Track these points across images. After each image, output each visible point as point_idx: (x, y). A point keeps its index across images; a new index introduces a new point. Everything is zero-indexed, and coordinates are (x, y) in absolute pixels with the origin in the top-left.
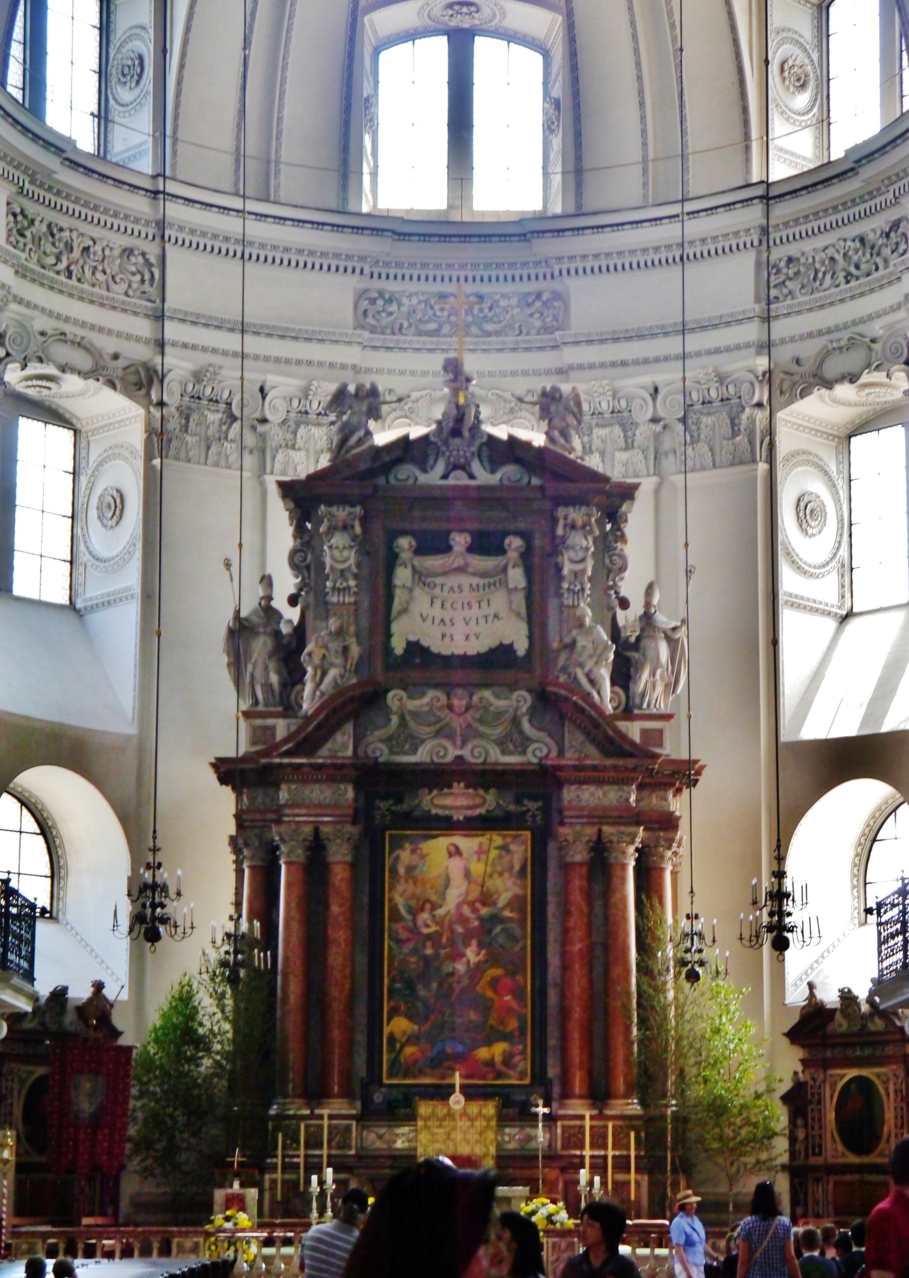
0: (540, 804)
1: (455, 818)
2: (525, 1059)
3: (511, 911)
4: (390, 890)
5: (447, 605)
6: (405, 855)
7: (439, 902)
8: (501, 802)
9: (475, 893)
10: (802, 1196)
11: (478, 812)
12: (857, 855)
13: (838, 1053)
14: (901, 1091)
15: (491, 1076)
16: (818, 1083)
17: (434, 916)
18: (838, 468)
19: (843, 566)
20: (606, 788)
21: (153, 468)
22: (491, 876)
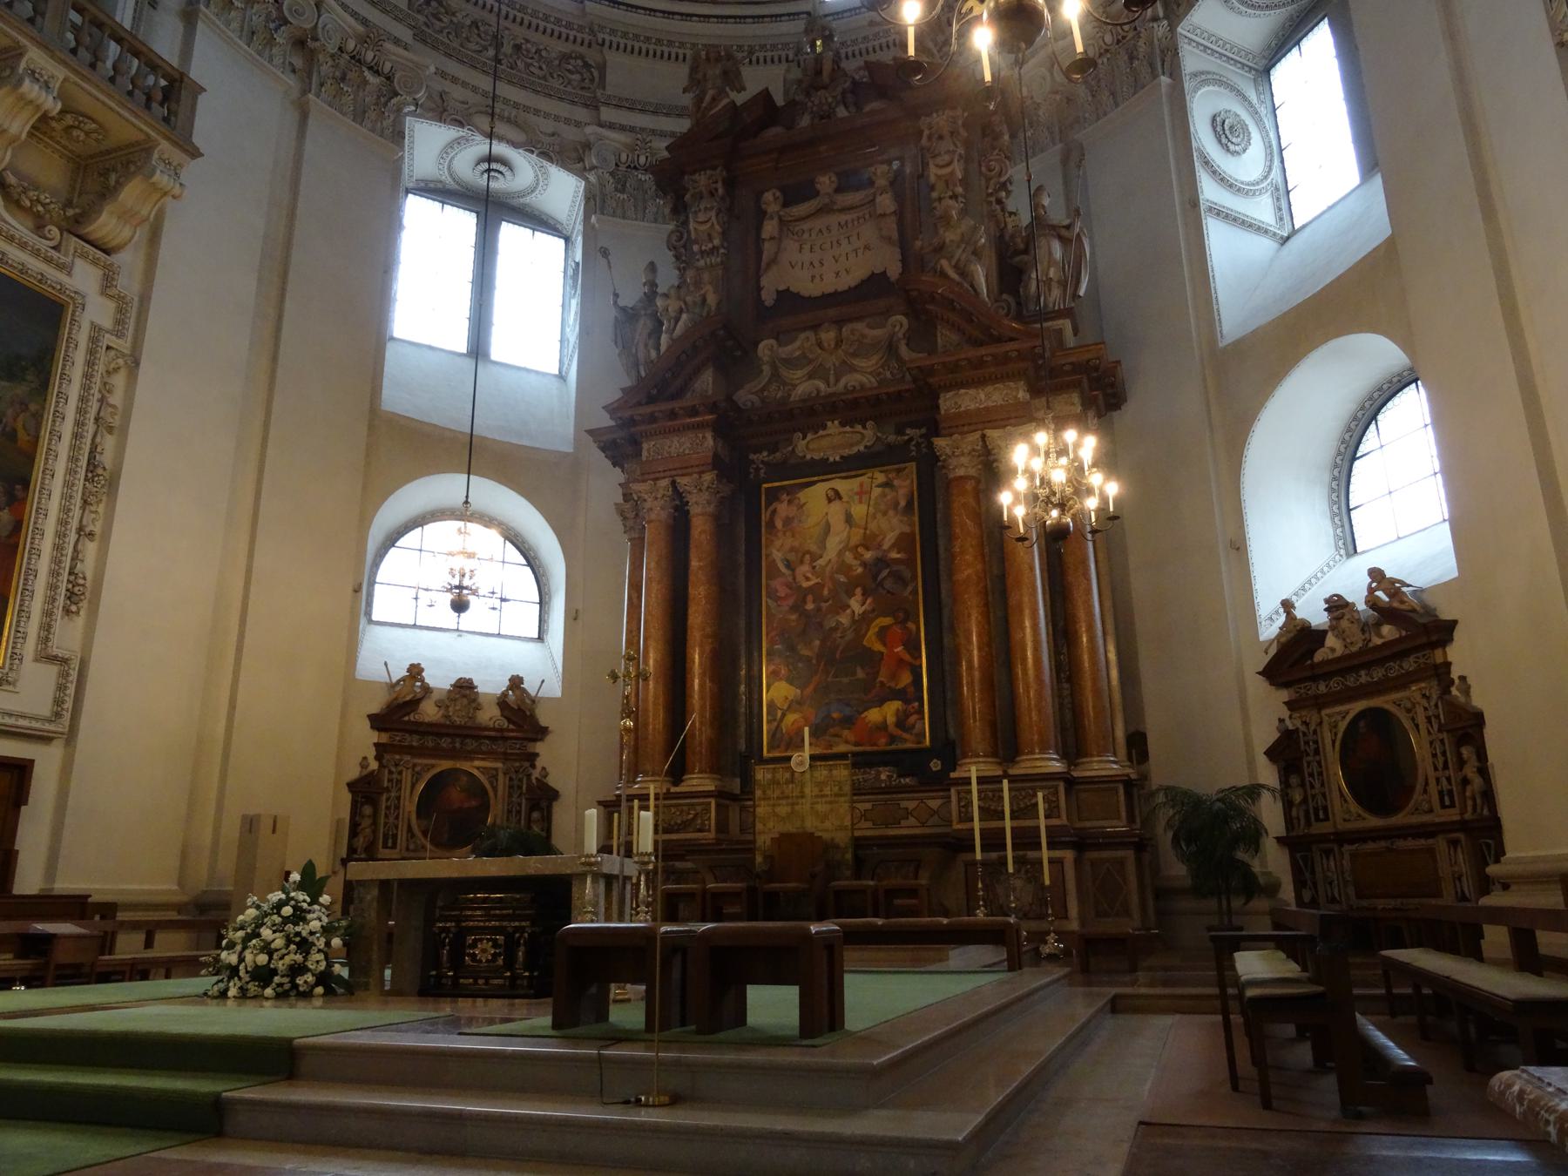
0: (923, 431)
1: (831, 459)
2: (923, 718)
3: (899, 553)
4: (767, 547)
5: (816, 248)
6: (783, 509)
7: (819, 552)
8: (879, 435)
9: (855, 540)
10: (1307, 875)
11: (855, 450)
12: (1334, 479)
13: (1335, 684)
14: (1437, 717)
15: (883, 741)
16: (1312, 727)
17: (814, 567)
18: (1259, 98)
19: (1277, 189)
20: (989, 389)
21: (593, 227)
22: (874, 517)
